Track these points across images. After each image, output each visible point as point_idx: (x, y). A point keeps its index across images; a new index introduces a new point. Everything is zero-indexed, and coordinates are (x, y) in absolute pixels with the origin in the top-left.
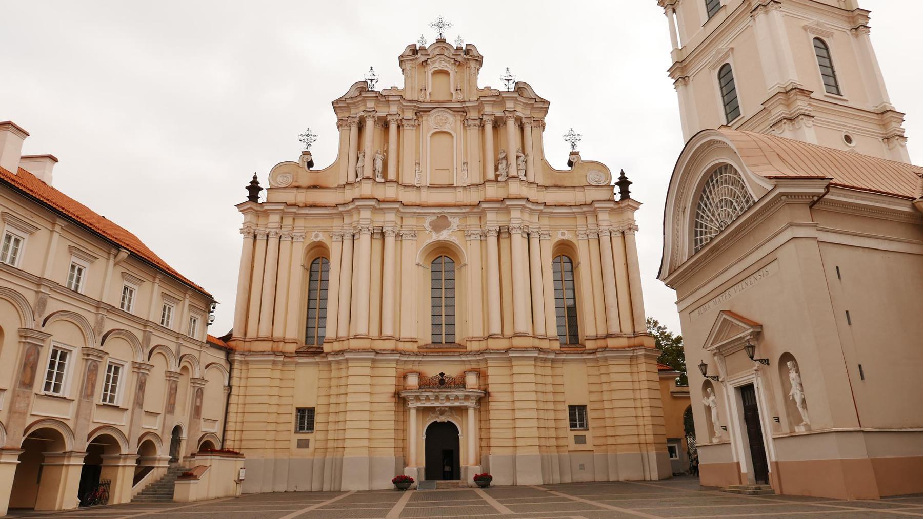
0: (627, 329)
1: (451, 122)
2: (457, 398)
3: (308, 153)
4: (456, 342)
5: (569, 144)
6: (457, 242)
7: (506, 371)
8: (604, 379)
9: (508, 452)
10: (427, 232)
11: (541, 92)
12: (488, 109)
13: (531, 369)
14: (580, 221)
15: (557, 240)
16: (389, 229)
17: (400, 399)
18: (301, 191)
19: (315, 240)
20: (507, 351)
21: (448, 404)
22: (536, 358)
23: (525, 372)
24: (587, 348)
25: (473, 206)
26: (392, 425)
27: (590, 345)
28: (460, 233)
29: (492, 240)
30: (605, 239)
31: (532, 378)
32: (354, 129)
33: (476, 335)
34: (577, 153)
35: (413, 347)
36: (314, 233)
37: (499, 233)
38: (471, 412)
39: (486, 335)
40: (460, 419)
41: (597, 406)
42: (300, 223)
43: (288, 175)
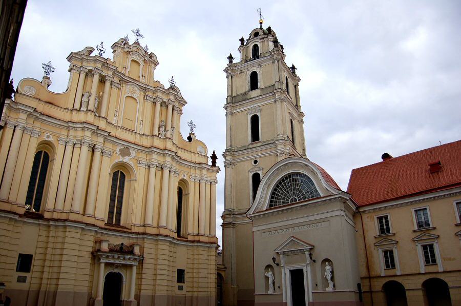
0: (207, 233)
1: (138, 94)
2: (129, 259)
3: (49, 78)
4: (121, 225)
5: (190, 128)
6: (133, 166)
7: (154, 247)
8: (196, 257)
9: (150, 293)
10: (117, 155)
11: (185, 94)
12: (160, 94)
13: (167, 248)
14: (193, 171)
15: (181, 178)
16: (100, 147)
17: (96, 255)
18: (41, 102)
19: (47, 139)
20: (157, 235)
21: (123, 262)
22: (170, 241)
23: (164, 247)
24: (189, 239)
25: (148, 148)
26: (88, 272)
27: (190, 238)
28: (135, 161)
29: (153, 170)
30: (203, 184)
31: (167, 252)
32: (83, 75)
33: (136, 223)
34: (194, 134)
35: (102, 224)
36: (46, 135)
37: (157, 166)
38: (134, 269)
39: (142, 224)
40: (125, 272)
41: (191, 270)
42: (38, 124)
43: (33, 89)
